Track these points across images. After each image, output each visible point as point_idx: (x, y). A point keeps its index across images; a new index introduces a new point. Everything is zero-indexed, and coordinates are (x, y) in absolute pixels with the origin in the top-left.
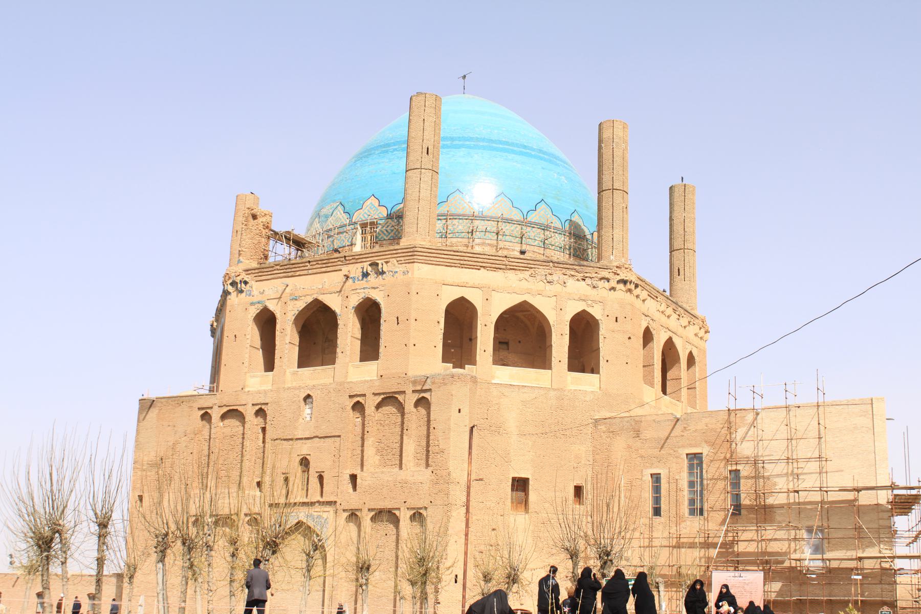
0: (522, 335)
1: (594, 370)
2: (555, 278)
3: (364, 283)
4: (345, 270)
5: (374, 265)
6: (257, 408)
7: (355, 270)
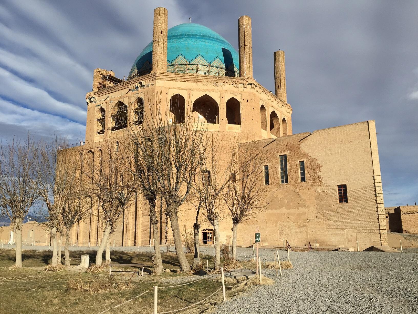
1: (239, 123)
2: (219, 84)
3: (137, 92)
5: (140, 83)
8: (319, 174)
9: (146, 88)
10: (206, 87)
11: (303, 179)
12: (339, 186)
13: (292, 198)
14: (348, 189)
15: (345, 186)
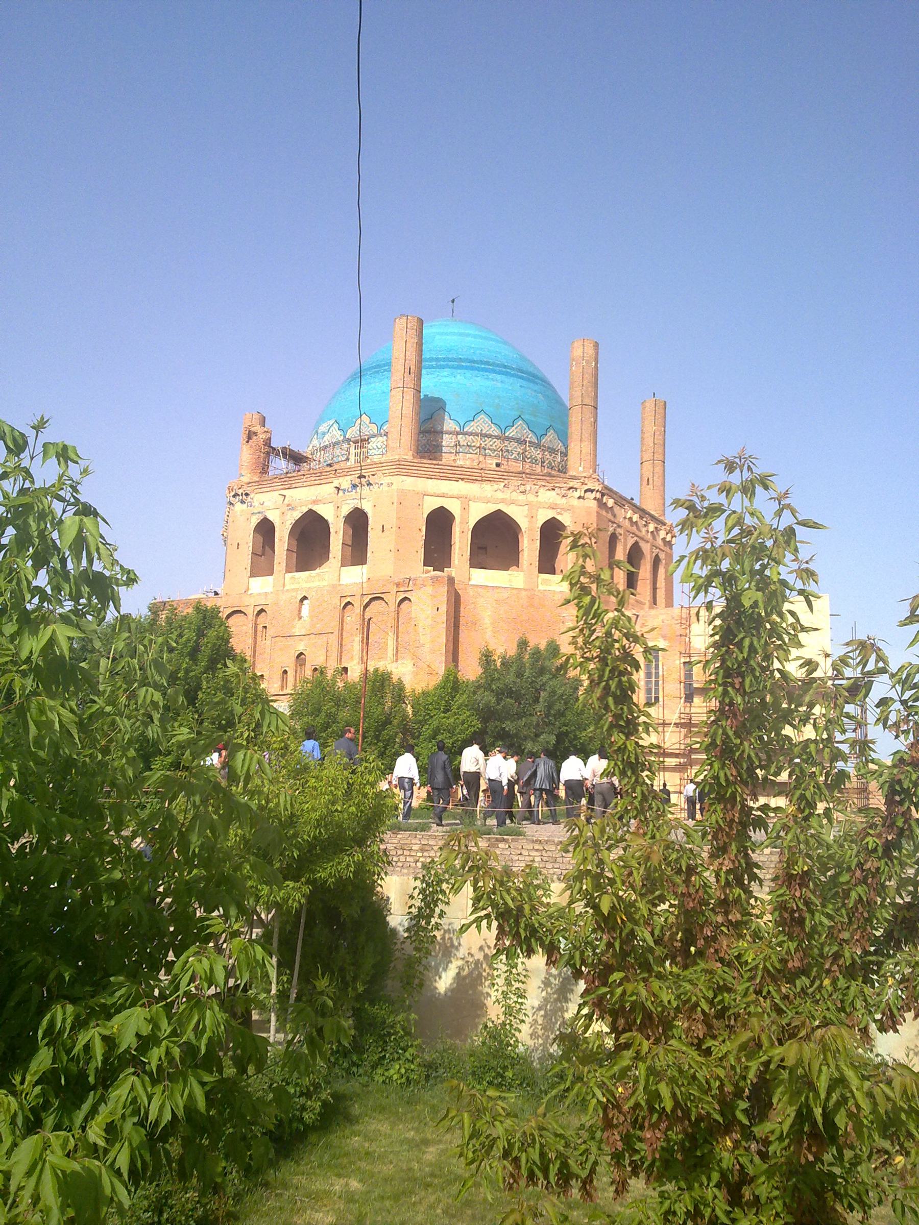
2: (528, 487)
4: (336, 483)
6: (259, 608)
7: (345, 483)
9: (375, 488)
10: (500, 495)
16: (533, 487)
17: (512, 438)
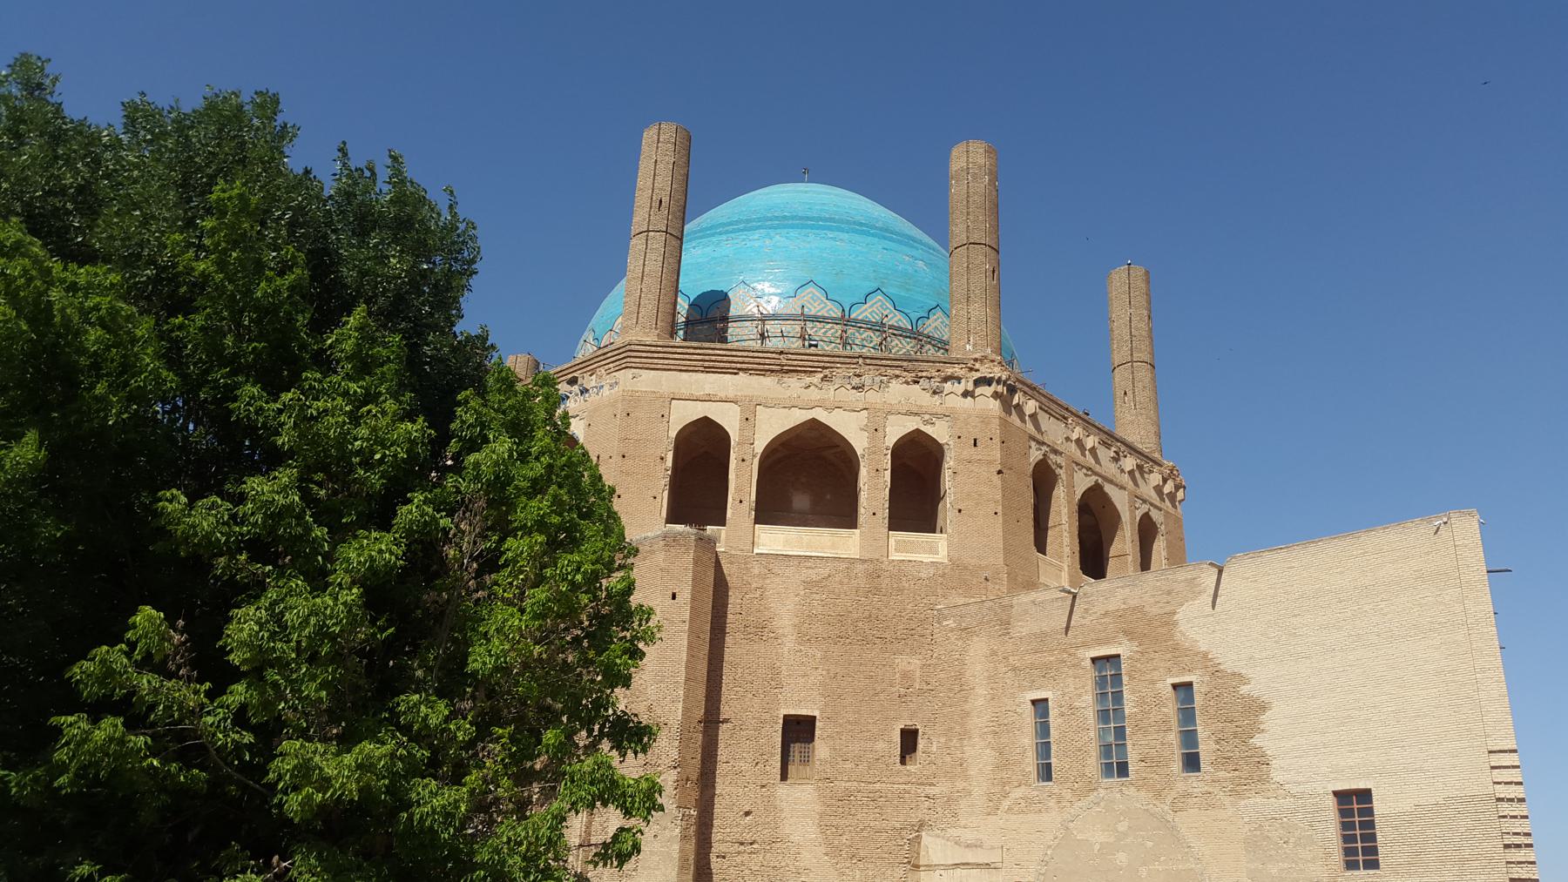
0: (809, 476)
2: (867, 379)
8: (1257, 741)
9: (592, 397)
11: (1192, 762)
12: (1342, 797)
13: (1150, 844)
14: (1379, 806)
15: (1365, 795)
16: (878, 379)
17: (862, 321)
